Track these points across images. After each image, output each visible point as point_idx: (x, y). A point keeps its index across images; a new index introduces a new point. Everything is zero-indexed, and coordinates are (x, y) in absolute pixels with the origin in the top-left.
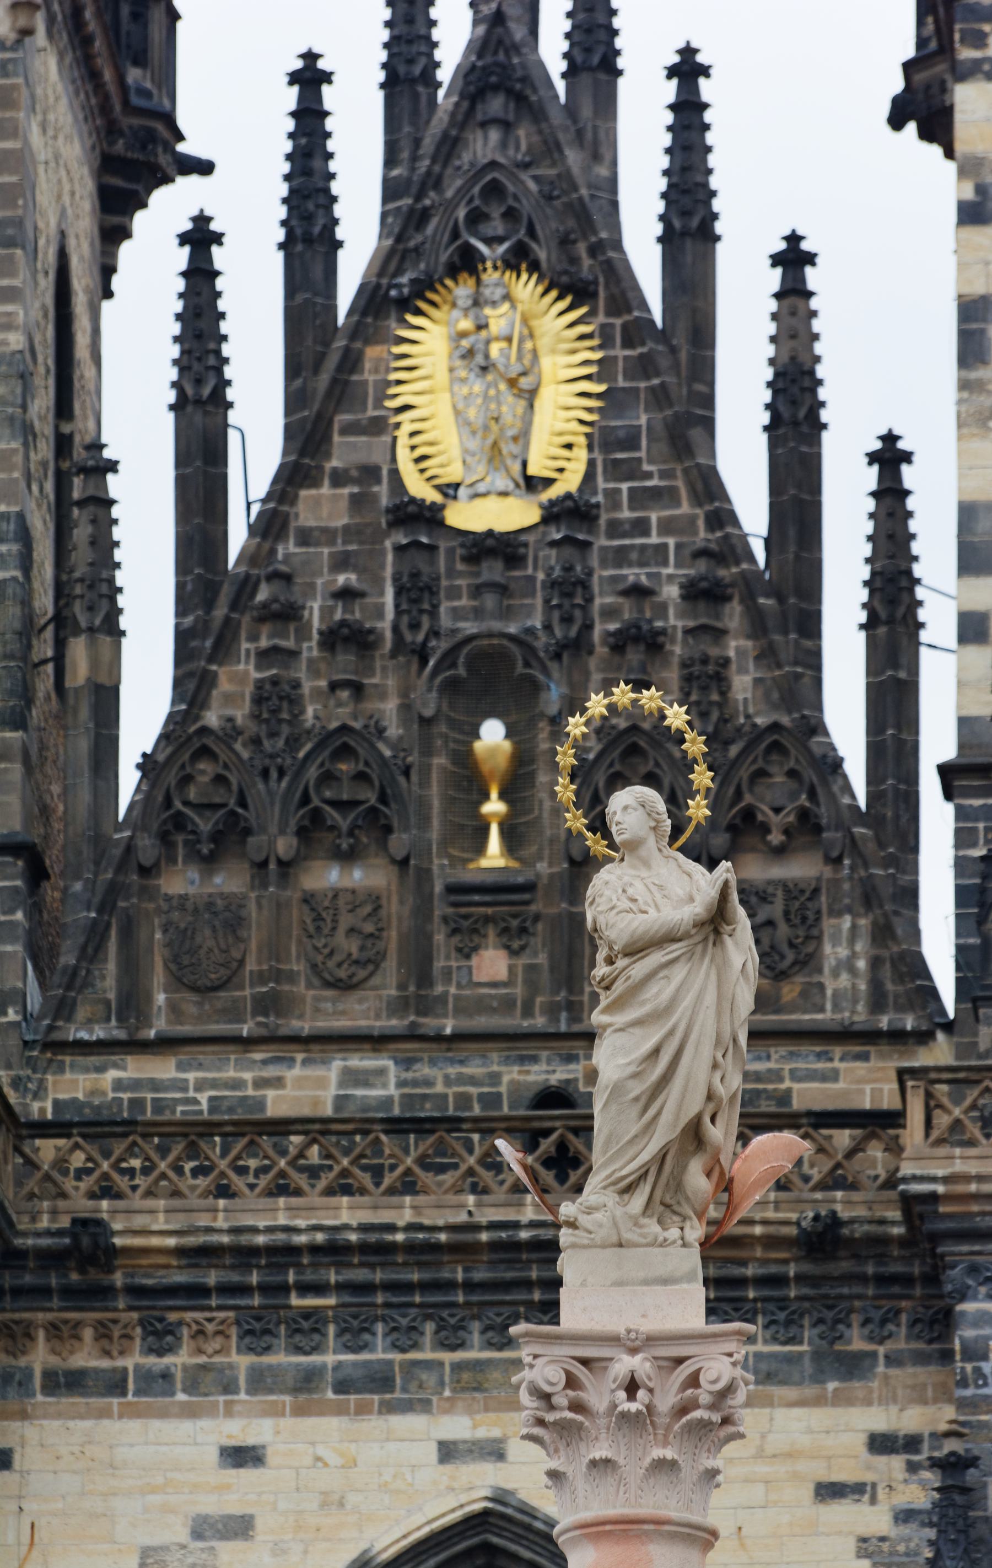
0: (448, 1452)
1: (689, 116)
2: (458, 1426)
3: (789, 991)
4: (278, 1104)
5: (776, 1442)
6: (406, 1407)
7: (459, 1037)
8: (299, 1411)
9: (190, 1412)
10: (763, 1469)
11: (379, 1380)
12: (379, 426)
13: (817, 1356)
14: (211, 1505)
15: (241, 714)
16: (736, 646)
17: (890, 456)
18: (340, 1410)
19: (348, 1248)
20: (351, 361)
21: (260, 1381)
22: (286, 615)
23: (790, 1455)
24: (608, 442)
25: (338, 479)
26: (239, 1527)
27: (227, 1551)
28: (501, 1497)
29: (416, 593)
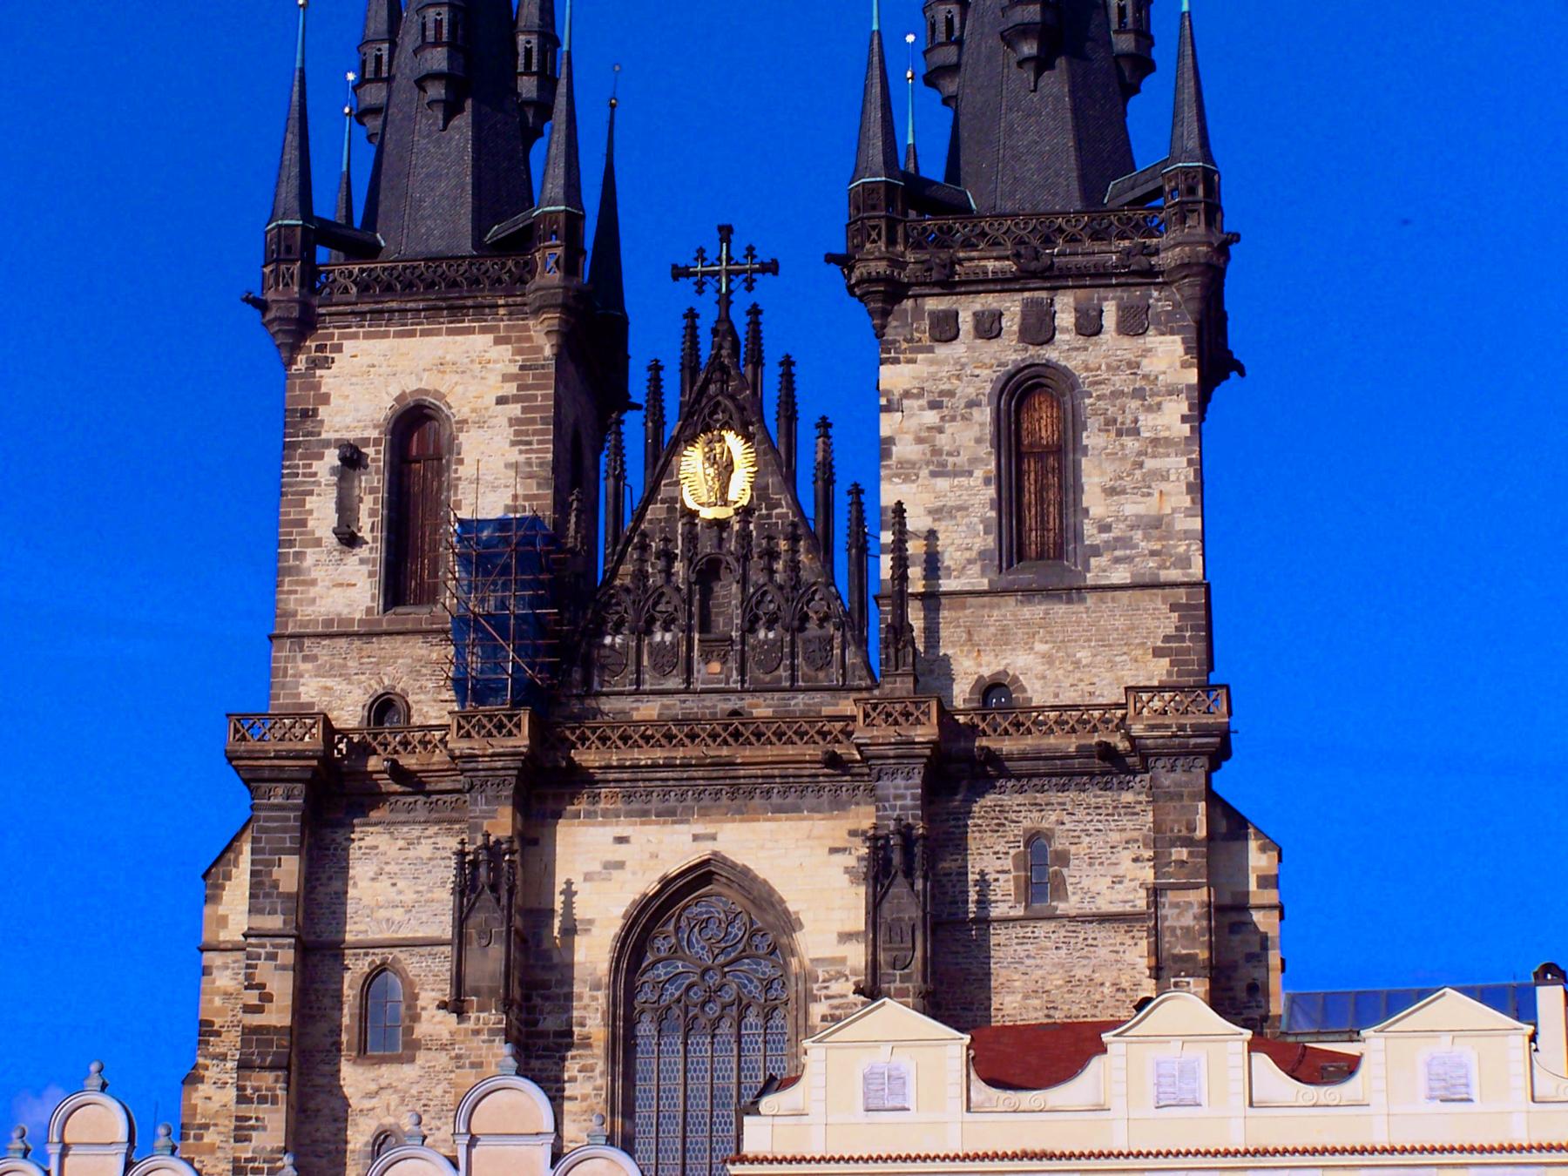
0: (696, 838)
1: (788, 379)
2: (700, 828)
3: (821, 675)
4: (636, 716)
5: (815, 833)
6: (681, 822)
7: (703, 692)
8: (643, 823)
9: (603, 824)
10: (810, 843)
11: (671, 813)
12: (677, 483)
13: (830, 802)
14: (611, 857)
15: (627, 581)
16: (803, 557)
17: (856, 491)
18: (657, 823)
19: (659, 766)
20: (667, 463)
21: (629, 814)
22: (643, 547)
23: (819, 838)
24: (759, 489)
25: (663, 501)
26: (620, 865)
27: (616, 874)
28: (715, 853)
29: (691, 538)
